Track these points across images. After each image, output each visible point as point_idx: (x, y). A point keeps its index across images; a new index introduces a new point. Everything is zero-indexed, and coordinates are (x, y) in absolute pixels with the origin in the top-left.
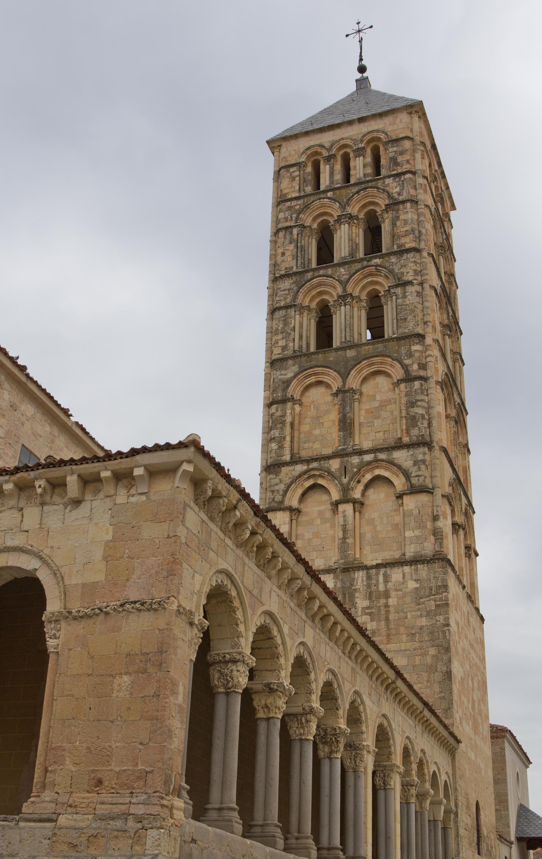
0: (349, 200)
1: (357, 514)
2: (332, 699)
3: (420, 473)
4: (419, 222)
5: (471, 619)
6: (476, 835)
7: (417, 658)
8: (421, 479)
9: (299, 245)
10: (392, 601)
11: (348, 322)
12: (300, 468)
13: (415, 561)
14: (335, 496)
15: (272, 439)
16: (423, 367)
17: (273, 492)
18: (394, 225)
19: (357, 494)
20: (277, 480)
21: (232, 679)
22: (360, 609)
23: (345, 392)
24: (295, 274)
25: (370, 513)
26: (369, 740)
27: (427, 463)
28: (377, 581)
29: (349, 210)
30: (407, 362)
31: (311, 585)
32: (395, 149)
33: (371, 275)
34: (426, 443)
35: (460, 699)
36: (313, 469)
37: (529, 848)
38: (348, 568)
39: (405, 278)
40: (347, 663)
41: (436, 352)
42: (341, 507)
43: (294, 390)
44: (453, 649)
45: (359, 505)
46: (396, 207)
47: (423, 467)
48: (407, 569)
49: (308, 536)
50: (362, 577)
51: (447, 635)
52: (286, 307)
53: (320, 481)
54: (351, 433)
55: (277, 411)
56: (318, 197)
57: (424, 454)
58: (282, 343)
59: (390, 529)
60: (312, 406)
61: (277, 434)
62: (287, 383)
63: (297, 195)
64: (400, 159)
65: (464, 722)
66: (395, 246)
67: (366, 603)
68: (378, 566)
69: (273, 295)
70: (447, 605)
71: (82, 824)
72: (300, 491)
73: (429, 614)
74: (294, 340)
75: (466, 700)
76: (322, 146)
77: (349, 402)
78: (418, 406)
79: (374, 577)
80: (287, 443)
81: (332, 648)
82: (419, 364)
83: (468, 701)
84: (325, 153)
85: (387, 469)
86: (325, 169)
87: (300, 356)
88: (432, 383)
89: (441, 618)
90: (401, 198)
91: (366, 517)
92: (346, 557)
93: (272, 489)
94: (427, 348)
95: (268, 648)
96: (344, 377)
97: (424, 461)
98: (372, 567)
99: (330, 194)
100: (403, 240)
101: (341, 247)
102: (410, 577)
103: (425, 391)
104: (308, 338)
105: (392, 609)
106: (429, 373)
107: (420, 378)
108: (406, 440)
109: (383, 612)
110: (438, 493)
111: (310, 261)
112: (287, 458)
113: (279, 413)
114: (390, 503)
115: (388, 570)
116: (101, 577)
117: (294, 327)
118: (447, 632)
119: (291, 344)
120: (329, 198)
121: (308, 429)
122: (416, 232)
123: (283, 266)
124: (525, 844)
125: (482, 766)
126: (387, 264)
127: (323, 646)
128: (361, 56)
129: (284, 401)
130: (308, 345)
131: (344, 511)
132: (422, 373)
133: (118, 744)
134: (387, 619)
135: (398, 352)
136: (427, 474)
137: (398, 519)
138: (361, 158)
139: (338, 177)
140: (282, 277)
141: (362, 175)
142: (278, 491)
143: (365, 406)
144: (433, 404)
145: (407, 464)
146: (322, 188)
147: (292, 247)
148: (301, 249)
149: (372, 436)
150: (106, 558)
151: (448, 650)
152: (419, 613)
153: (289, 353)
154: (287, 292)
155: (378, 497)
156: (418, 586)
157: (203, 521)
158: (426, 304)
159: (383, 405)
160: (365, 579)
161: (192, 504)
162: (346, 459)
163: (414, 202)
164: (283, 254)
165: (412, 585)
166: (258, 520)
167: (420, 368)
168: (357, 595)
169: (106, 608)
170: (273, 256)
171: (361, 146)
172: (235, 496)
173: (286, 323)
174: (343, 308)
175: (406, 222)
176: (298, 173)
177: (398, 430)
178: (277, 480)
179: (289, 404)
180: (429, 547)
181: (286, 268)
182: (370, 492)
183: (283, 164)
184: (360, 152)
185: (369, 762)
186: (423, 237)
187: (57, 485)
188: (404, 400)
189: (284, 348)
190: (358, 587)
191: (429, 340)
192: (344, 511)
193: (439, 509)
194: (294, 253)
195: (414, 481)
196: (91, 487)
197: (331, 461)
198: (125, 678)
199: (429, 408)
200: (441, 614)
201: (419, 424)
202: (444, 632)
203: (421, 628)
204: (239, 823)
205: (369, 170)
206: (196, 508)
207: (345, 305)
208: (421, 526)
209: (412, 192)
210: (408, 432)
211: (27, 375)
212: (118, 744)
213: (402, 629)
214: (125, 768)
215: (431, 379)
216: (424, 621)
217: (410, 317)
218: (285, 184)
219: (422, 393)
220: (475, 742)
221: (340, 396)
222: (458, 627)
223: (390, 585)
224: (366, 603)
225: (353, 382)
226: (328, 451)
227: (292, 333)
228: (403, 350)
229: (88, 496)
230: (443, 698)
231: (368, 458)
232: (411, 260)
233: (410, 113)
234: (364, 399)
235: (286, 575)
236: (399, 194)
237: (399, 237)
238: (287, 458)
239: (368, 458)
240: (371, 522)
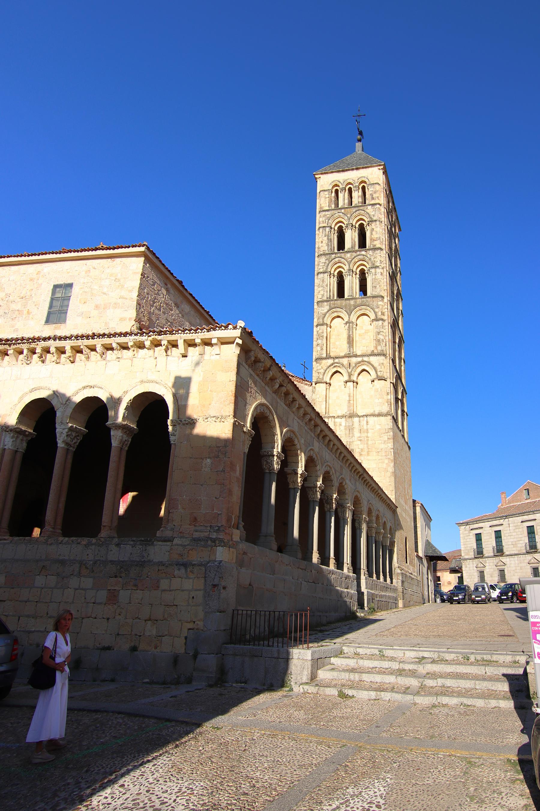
3: (381, 370)
8: (382, 373)
12: (330, 361)
14: (346, 378)
17: (318, 373)
19: (354, 378)
29: (351, 221)
30: (376, 310)
47: (383, 367)
53: (339, 370)
58: (322, 293)
72: (330, 374)
96: (349, 315)
97: (383, 364)
112: (324, 356)
113: (320, 331)
132: (382, 317)
139: (346, 201)
145: (376, 365)
147: (326, 238)
148: (330, 240)
153: (325, 298)
155: (364, 379)
162: (350, 359)
164: (322, 242)
178: (320, 367)
189: (323, 295)
197: (344, 359)
205: (360, 200)
217: (378, 286)
221: (348, 325)
225: (353, 318)
226: (342, 354)
231: (360, 359)
236: (374, 216)
238: (324, 356)
239: (360, 359)
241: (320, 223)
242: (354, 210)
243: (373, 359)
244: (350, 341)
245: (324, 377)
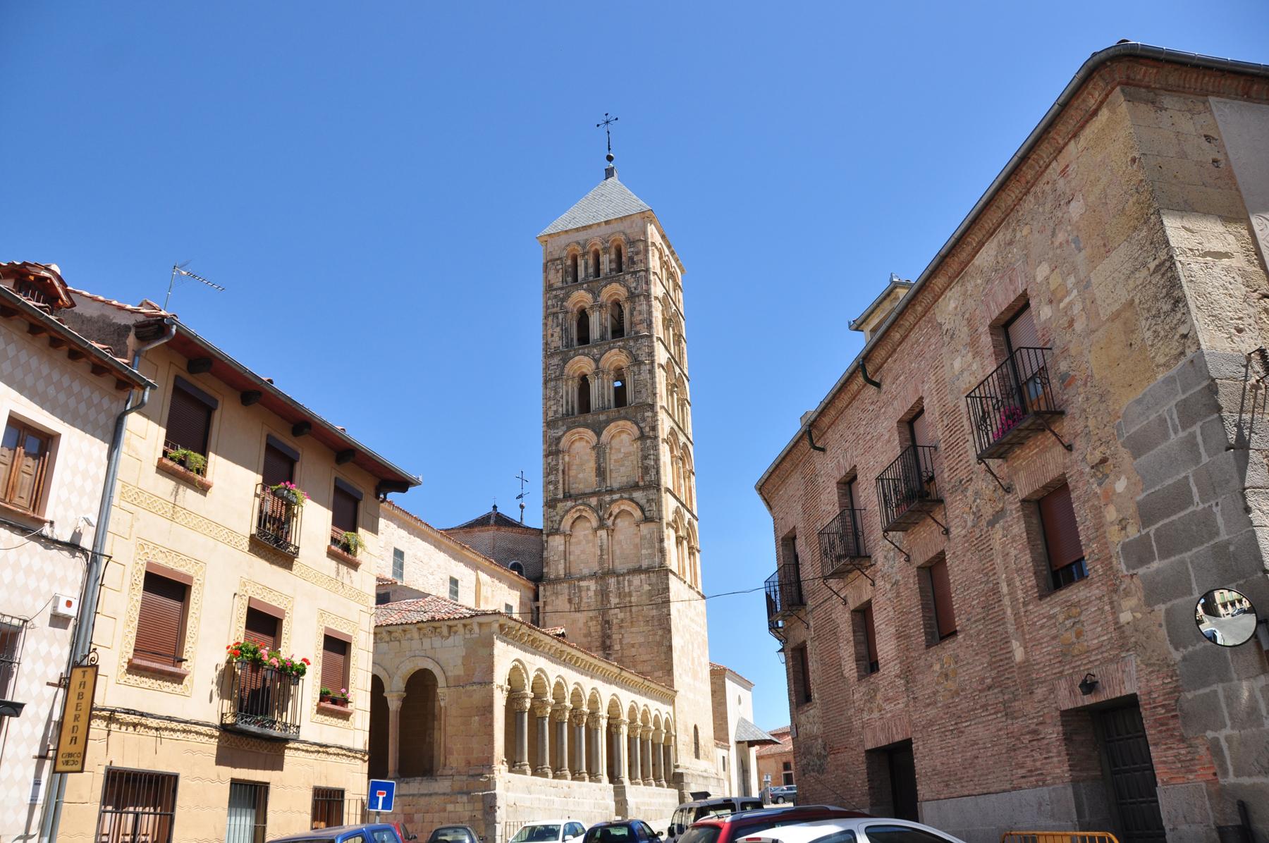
4: (650, 313)
12: (570, 504)
13: (647, 571)
15: (550, 483)
16: (654, 428)
18: (632, 314)
25: (619, 536)
26: (603, 712)
30: (642, 425)
34: (656, 485)
38: (602, 576)
42: (599, 533)
43: (564, 443)
48: (643, 576)
52: (557, 379)
58: (554, 408)
63: (560, 285)
67: (617, 600)
69: (546, 368)
70: (669, 601)
76: (578, 243)
80: (560, 486)
86: (581, 262)
89: (665, 610)
94: (655, 414)
96: (599, 434)
100: (638, 328)
101: (595, 332)
103: (656, 448)
107: (649, 437)
114: (633, 529)
116: (462, 673)
123: (553, 345)
137: (638, 540)
139: (591, 270)
140: (552, 355)
143: (614, 457)
145: (643, 502)
147: (558, 329)
148: (565, 331)
151: (670, 631)
153: (559, 416)
159: (627, 455)
163: (648, 296)
165: (646, 587)
170: (545, 336)
173: (556, 393)
175: (640, 313)
177: (636, 475)
182: (618, 521)
184: (606, 250)
185: (604, 723)
188: (640, 454)
189: (556, 412)
195: (647, 514)
199: (657, 460)
205: (614, 266)
208: (652, 547)
216: (654, 612)
218: (552, 276)
224: (617, 600)
231: (616, 496)
238: (561, 496)
240: (620, 542)
243: (637, 495)
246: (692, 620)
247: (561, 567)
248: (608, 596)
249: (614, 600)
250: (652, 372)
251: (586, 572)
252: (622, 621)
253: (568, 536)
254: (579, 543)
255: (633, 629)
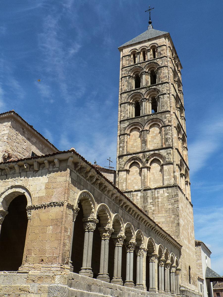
0: (145, 66)
1: (148, 171)
2: (130, 233)
5: (188, 205)
6: (189, 277)
7: (168, 219)
9: (129, 82)
10: (160, 200)
11: (145, 107)
12: (129, 157)
16: (170, 122)
17: (121, 164)
19: (148, 165)
20: (122, 161)
21: (90, 227)
22: (149, 203)
23: (144, 131)
24: (128, 92)
27: (171, 154)
28: (155, 193)
30: (164, 120)
31: (120, 195)
32: (160, 49)
33: (153, 91)
35: (183, 232)
36: (134, 157)
37: (211, 281)
39: (164, 92)
40: (136, 221)
41: (174, 117)
44: (180, 215)
45: (149, 168)
46: (161, 68)
47: (170, 155)
48: (165, 189)
49: (132, 179)
50: (150, 192)
51: (178, 211)
54: (146, 144)
55: (122, 137)
56: (135, 66)
57: (170, 151)
58: (123, 115)
59: (159, 176)
60: (133, 136)
61: (122, 145)
62: (125, 128)
63: (128, 65)
64: (162, 52)
65: (184, 240)
66: (160, 81)
67: (151, 201)
68: (155, 189)
70: (178, 201)
71: (36, 274)
73: (172, 204)
74: (127, 114)
75: (185, 233)
76: (136, 49)
77: (145, 134)
78: (168, 135)
79: (154, 192)
81: (129, 216)
82: (168, 121)
83: (186, 233)
84: (137, 51)
85: (158, 156)
87: (129, 119)
88: (173, 127)
89: (176, 205)
90: (162, 65)
91: (151, 172)
92: (145, 186)
93: (120, 163)
95: (105, 217)
98: (153, 189)
99: (139, 65)
100: (163, 80)
102: (166, 192)
104: (132, 113)
105: (160, 203)
106: (172, 124)
108: (164, 146)
109: (157, 204)
110: (175, 164)
111: (132, 87)
112: (125, 153)
113: (123, 138)
115: (158, 190)
116: (44, 195)
117: (127, 110)
118: (178, 210)
119: (126, 115)
120: (138, 66)
121: (132, 143)
122: (168, 77)
124: (209, 280)
125: (192, 254)
126: (158, 88)
127: (126, 216)
128: (150, 18)
129: (124, 134)
130: (132, 115)
131: (144, 170)
132: (170, 124)
133: (48, 248)
134: (158, 206)
135: (161, 117)
136: (171, 157)
138: (149, 52)
140: (123, 93)
141: (149, 58)
142: (122, 164)
144: (173, 134)
146: (136, 63)
147: (126, 83)
149: (153, 145)
150: (46, 188)
151: (178, 216)
152: (169, 204)
153: (126, 118)
154: (125, 98)
156: (168, 195)
157: (78, 176)
158: (171, 101)
160: (151, 193)
161: (74, 170)
164: (124, 85)
165: (166, 194)
166: (99, 175)
167: (169, 122)
168: (148, 198)
169: (45, 204)
171: (149, 48)
172: (89, 168)
174: (143, 103)
176: (128, 58)
178: (122, 161)
179: (126, 135)
180: (172, 182)
181: (125, 90)
183: (124, 56)
186: (170, 78)
187: (31, 166)
189: (124, 117)
190: (148, 195)
191: (172, 113)
192: (144, 170)
193: (175, 169)
194: (127, 85)
195: (167, 160)
196: (42, 166)
198: (51, 227)
200: (176, 204)
201: (168, 141)
202: (177, 210)
203: (169, 209)
204: (92, 274)
205: (152, 56)
206: (76, 172)
207: (144, 102)
208: (170, 175)
209: (166, 63)
210: (165, 144)
211: (33, 129)
212: (48, 248)
213: (163, 209)
214: (50, 256)
215: (172, 126)
216: (170, 207)
219: (170, 130)
220: (189, 246)
222: (182, 208)
223: (159, 195)
224: (151, 201)
226: (139, 151)
227: (127, 112)
228: (163, 116)
229: (41, 169)
230: (176, 232)
231: (152, 153)
232: (166, 86)
233: (165, 37)
234: (150, 133)
235: (111, 193)
237: (162, 78)
239: (152, 153)
240: (153, 174)
241: (122, 75)
242: (148, 63)
243: (163, 152)
244: (144, 142)
245: (125, 167)
246: (187, 214)
247: (124, 185)
248: (147, 199)
249: (150, 201)
250: (169, 97)
251: (136, 188)
252: (154, 211)
253: (128, 171)
254: (133, 174)
255: (159, 215)
